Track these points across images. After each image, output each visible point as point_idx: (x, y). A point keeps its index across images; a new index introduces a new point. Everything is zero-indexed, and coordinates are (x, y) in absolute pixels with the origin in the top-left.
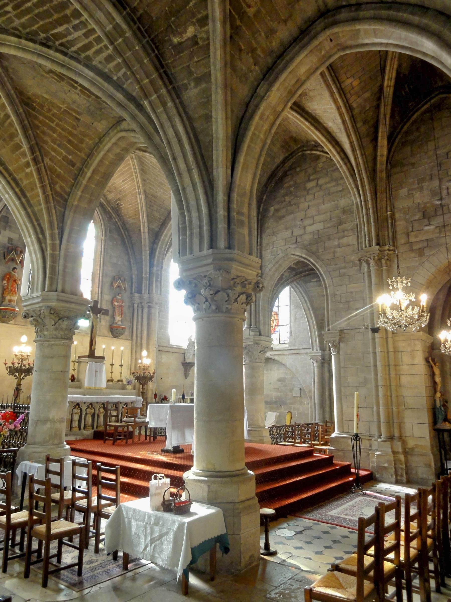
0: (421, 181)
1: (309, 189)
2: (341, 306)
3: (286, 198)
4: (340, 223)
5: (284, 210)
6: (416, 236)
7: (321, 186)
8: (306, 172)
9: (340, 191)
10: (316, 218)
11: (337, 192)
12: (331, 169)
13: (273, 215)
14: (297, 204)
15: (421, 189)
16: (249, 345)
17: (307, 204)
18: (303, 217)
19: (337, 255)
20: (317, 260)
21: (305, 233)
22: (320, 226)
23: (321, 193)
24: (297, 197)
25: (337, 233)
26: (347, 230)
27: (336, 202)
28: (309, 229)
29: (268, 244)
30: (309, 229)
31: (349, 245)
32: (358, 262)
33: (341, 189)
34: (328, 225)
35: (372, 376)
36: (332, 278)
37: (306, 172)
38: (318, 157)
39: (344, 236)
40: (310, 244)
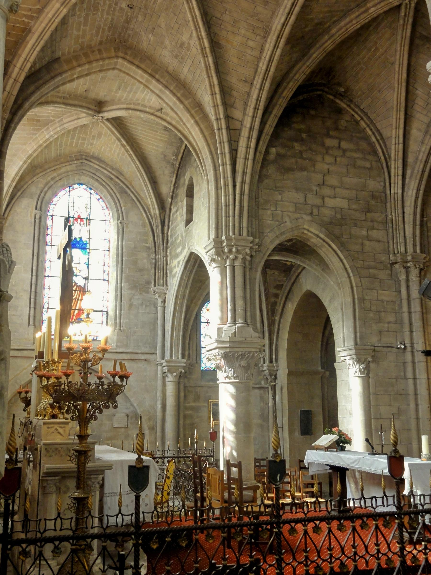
2: (372, 315)
3: (296, 144)
5: (293, 160)
9: (369, 169)
10: (337, 190)
11: (365, 168)
12: (358, 135)
14: (313, 162)
16: (249, 353)
17: (326, 167)
18: (321, 182)
20: (341, 248)
21: (323, 206)
23: (344, 161)
24: (310, 149)
25: (365, 220)
26: (377, 222)
27: (363, 180)
29: (267, 202)
30: (330, 202)
31: (379, 241)
32: (389, 266)
33: (369, 166)
34: (354, 207)
35: (412, 406)
36: (360, 277)
38: (339, 111)
39: (373, 228)
40: (331, 223)
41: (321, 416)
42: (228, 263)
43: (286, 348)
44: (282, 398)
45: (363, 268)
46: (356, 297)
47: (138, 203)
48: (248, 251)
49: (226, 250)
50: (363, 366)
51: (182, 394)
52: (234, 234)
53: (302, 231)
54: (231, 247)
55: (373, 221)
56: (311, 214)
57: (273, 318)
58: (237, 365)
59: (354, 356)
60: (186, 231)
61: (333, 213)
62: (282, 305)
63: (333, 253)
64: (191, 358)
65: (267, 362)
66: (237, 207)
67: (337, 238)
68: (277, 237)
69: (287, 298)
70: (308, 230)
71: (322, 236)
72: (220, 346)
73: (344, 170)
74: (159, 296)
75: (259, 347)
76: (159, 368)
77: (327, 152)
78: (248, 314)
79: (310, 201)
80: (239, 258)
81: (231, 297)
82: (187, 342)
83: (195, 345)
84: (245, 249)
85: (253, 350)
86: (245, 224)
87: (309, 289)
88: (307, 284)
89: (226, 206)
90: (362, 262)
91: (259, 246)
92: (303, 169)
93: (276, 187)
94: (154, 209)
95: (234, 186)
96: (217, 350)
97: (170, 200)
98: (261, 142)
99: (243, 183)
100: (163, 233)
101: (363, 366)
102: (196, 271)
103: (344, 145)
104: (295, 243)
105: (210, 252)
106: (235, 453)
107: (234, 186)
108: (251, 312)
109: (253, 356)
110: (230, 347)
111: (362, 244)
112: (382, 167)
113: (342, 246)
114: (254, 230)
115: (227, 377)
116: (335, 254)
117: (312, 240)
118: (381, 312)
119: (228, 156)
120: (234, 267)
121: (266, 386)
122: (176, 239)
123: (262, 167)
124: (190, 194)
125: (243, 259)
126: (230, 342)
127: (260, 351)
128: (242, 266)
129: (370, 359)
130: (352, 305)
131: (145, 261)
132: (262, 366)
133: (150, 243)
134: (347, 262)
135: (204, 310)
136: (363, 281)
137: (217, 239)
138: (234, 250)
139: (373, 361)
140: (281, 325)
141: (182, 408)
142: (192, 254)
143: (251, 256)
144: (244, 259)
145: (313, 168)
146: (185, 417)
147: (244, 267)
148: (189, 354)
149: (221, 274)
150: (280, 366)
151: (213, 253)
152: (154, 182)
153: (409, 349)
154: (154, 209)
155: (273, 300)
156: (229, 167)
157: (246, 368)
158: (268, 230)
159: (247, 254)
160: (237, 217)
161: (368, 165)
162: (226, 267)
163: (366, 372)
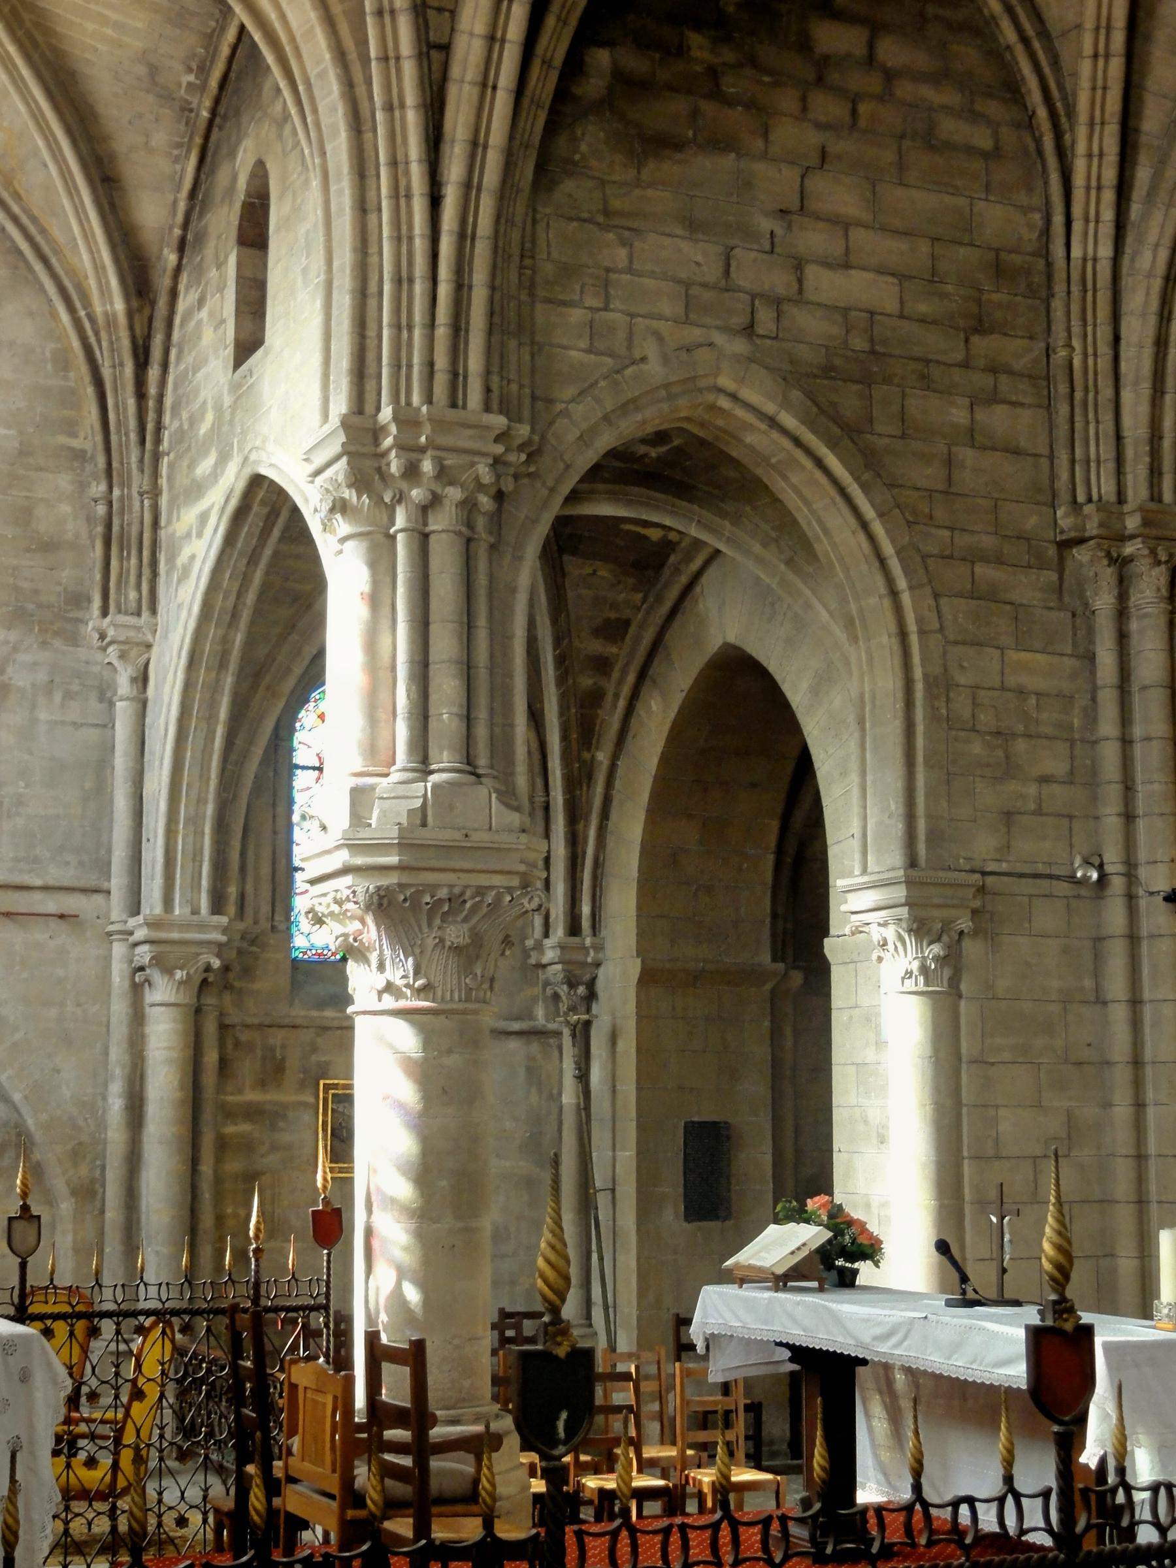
3: (696, 41)
5: (679, 105)
9: (985, 155)
10: (859, 236)
12: (946, 13)
16: (481, 891)
18: (793, 202)
20: (866, 476)
21: (799, 297)
22: (882, 294)
24: (753, 62)
25: (966, 365)
26: (1010, 372)
27: (961, 202)
29: (568, 272)
30: (823, 284)
31: (1016, 452)
32: (1052, 551)
33: (986, 144)
34: (923, 308)
35: (1122, 1112)
36: (936, 596)
39: (994, 398)
40: (828, 371)
41: (767, 1147)
42: (401, 520)
43: (635, 874)
44: (615, 1072)
45: (951, 557)
46: (918, 674)
47: (38, 267)
48: (484, 471)
49: (395, 466)
50: (936, 949)
51: (211, 1057)
52: (429, 399)
53: (710, 397)
54: (414, 455)
55: (993, 369)
56: (749, 330)
57: (586, 756)
58: (430, 942)
59: (904, 912)
60: (235, 387)
61: (836, 330)
62: (622, 703)
63: (833, 492)
64: (249, 911)
65: (559, 932)
66: (444, 290)
67: (849, 434)
68: (606, 418)
69: (642, 674)
70: (734, 397)
71: (789, 421)
72: (359, 861)
73: (889, 156)
74: (122, 656)
75: (522, 868)
76: (119, 949)
77: (820, 79)
78: (481, 732)
79: (743, 278)
80: (447, 502)
81: (411, 662)
82: (236, 843)
83: (266, 854)
84: (473, 464)
85: (497, 880)
86: (475, 362)
87: (731, 639)
88: (726, 618)
89: (398, 281)
90: (947, 533)
91: (529, 456)
92: (720, 144)
93: (607, 213)
94: (104, 291)
95: (435, 201)
96: (348, 880)
97: (172, 258)
98: (551, 21)
99: (469, 187)
100: (141, 395)
101: (936, 949)
102: (276, 554)
103: (891, 51)
104: (678, 450)
105: (329, 473)
106: (412, 1295)
107: (435, 201)
108: (492, 725)
109: (496, 905)
110: (401, 868)
111: (949, 462)
112: (1040, 152)
113: (870, 463)
114: (514, 387)
115: (389, 988)
116: (839, 500)
117: (749, 439)
118: (1014, 736)
119: (409, 69)
120: (426, 536)
121: (552, 1026)
122: (193, 421)
123: (552, 128)
124: (254, 235)
125: (462, 504)
126: (404, 844)
127: (525, 885)
128: (459, 533)
129: (965, 923)
130: (900, 706)
131: (65, 508)
132: (539, 947)
133: (88, 438)
134: (887, 532)
135: (307, 717)
136: (946, 610)
137: (357, 420)
138: (427, 466)
139: (976, 933)
140: (618, 784)
141: (208, 1115)
142: (257, 481)
143: (500, 496)
144: (468, 506)
145: (760, 143)
146: (222, 1145)
147: (469, 541)
148: (242, 896)
149: (373, 564)
150: (608, 946)
151: (341, 478)
152: (106, 179)
153: (1117, 884)
154: (104, 291)
155: (586, 681)
156: (413, 119)
157: (467, 955)
158: (570, 392)
159: (480, 487)
160: (442, 332)
161: (982, 139)
162: (393, 538)
163: (947, 973)
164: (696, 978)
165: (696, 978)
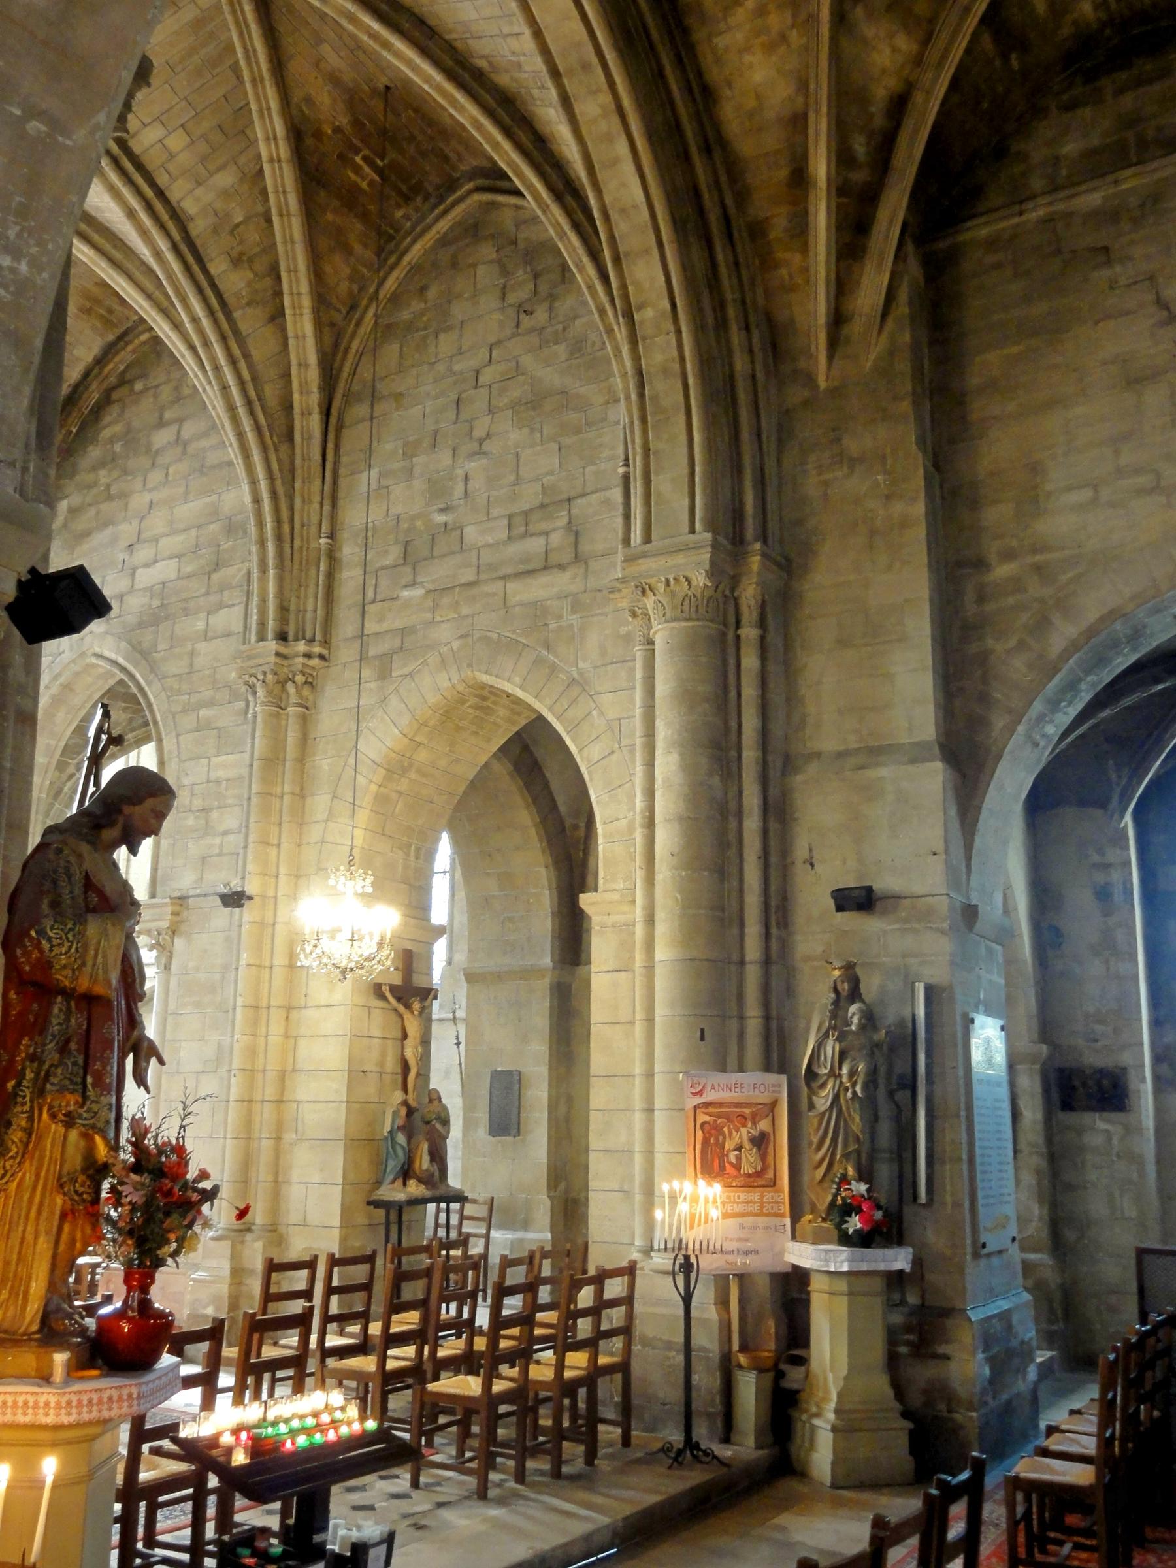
0: (410, 451)
1: (157, 452)
3: (102, 473)
4: (217, 566)
6: (381, 620)
7: (185, 445)
8: (155, 396)
10: (163, 542)
13: (65, 526)
14: (124, 496)
15: (409, 472)
19: (199, 662)
20: (151, 677)
22: (166, 570)
23: (183, 467)
25: (207, 593)
27: (214, 498)
28: (145, 577)
34: (189, 569)
36: (178, 735)
37: (155, 396)
40: (141, 625)
61: (146, 600)
118: (211, 809)
164: (499, 977)
165: (499, 977)
